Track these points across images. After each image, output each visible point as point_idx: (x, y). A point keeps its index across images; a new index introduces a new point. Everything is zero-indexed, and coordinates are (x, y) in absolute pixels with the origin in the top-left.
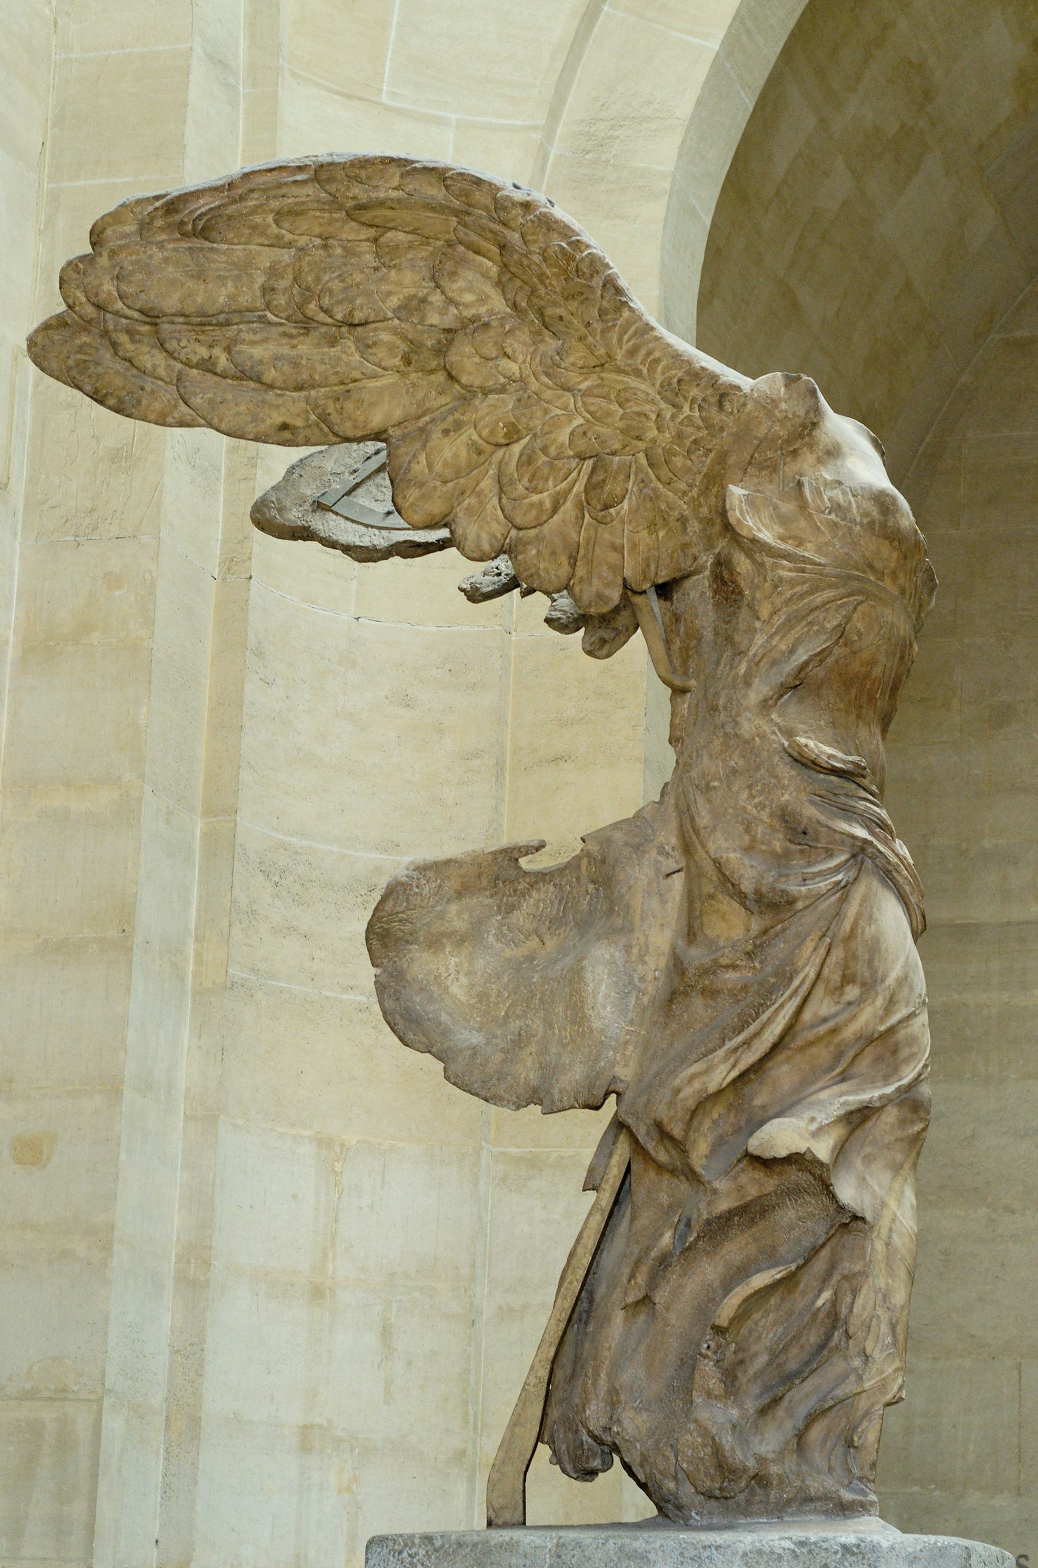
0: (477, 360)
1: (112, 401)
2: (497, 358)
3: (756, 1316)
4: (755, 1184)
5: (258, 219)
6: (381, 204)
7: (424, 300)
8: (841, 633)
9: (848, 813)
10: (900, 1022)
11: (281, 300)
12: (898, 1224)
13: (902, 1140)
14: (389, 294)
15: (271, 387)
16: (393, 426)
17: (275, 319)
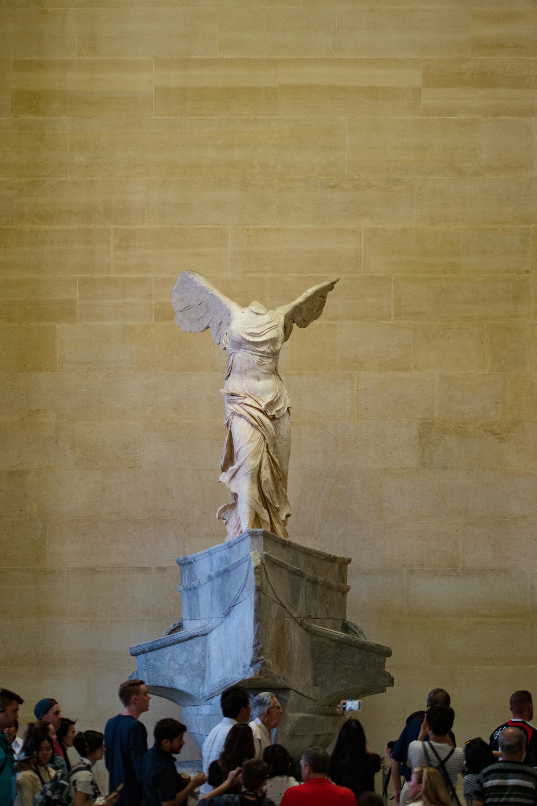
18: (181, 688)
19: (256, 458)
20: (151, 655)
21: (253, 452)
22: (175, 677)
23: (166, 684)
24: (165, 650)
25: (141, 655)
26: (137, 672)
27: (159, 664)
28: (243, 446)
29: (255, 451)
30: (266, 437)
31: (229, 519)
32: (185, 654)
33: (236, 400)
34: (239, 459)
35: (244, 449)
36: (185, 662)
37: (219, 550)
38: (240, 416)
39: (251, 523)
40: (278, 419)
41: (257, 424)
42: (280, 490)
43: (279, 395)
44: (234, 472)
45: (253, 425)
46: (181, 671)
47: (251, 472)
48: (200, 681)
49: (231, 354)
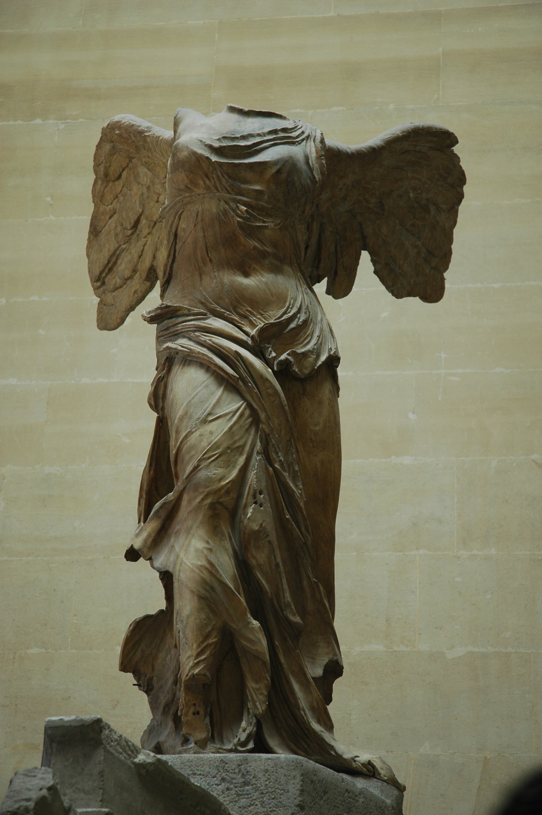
0: (156, 205)
1: (109, 327)
2: (158, 198)
3: (161, 655)
5: (101, 209)
6: (106, 169)
7: (142, 194)
8: (176, 235)
9: (176, 335)
10: (181, 442)
11: (120, 236)
12: (183, 565)
13: (190, 512)
14: (135, 201)
15: (131, 278)
16: (153, 261)
17: (124, 246)
19: (229, 465)
21: (216, 446)
28: (190, 433)
29: (225, 445)
30: (263, 416)
34: (180, 474)
35: (193, 439)
38: (189, 359)
39: (208, 653)
40: (303, 380)
41: (230, 371)
42: (305, 583)
43: (302, 317)
44: (163, 514)
45: (221, 379)
47: (209, 501)
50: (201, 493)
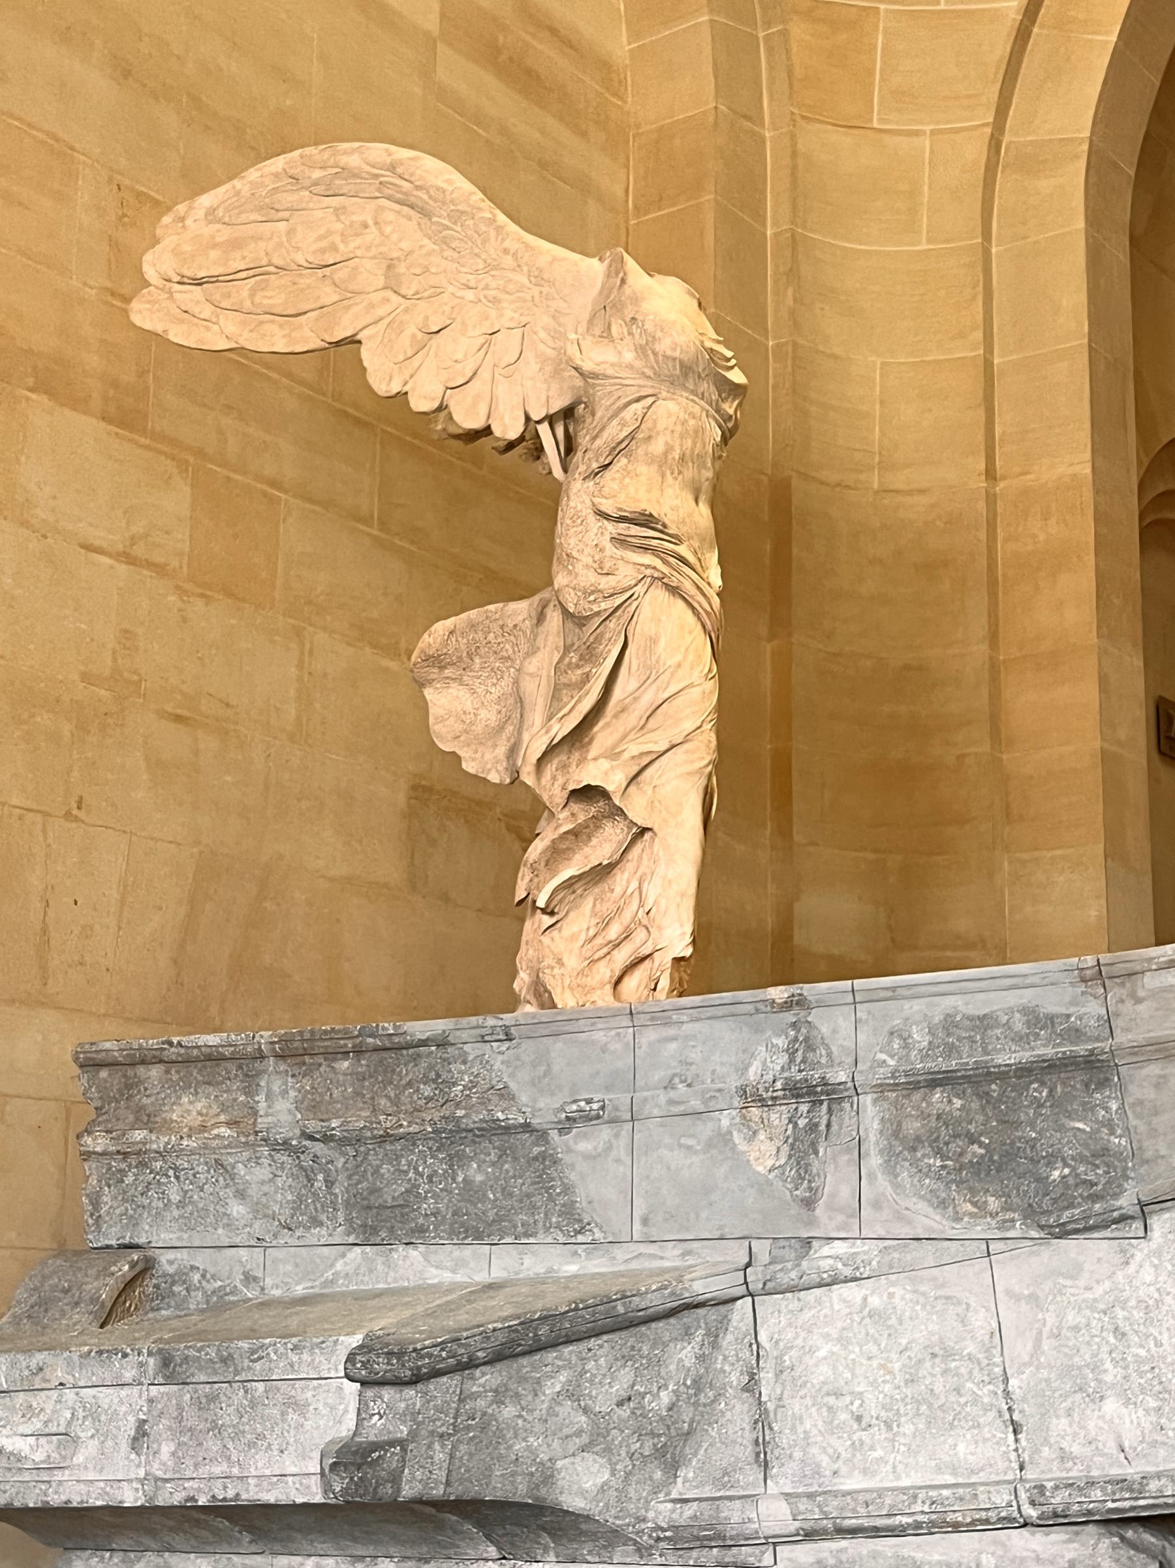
4: (582, 812)
18: (574, 1503)
20: (487, 1378)
22: (559, 1464)
23: (520, 1492)
24: (551, 1356)
25: (445, 1379)
26: (402, 1443)
27: (509, 1411)
31: (567, 912)
32: (626, 1375)
33: (654, 542)
36: (620, 1404)
37: (923, 989)
38: (674, 591)
46: (597, 1441)
48: (658, 1475)
49: (638, 400)
50: (703, 758)
